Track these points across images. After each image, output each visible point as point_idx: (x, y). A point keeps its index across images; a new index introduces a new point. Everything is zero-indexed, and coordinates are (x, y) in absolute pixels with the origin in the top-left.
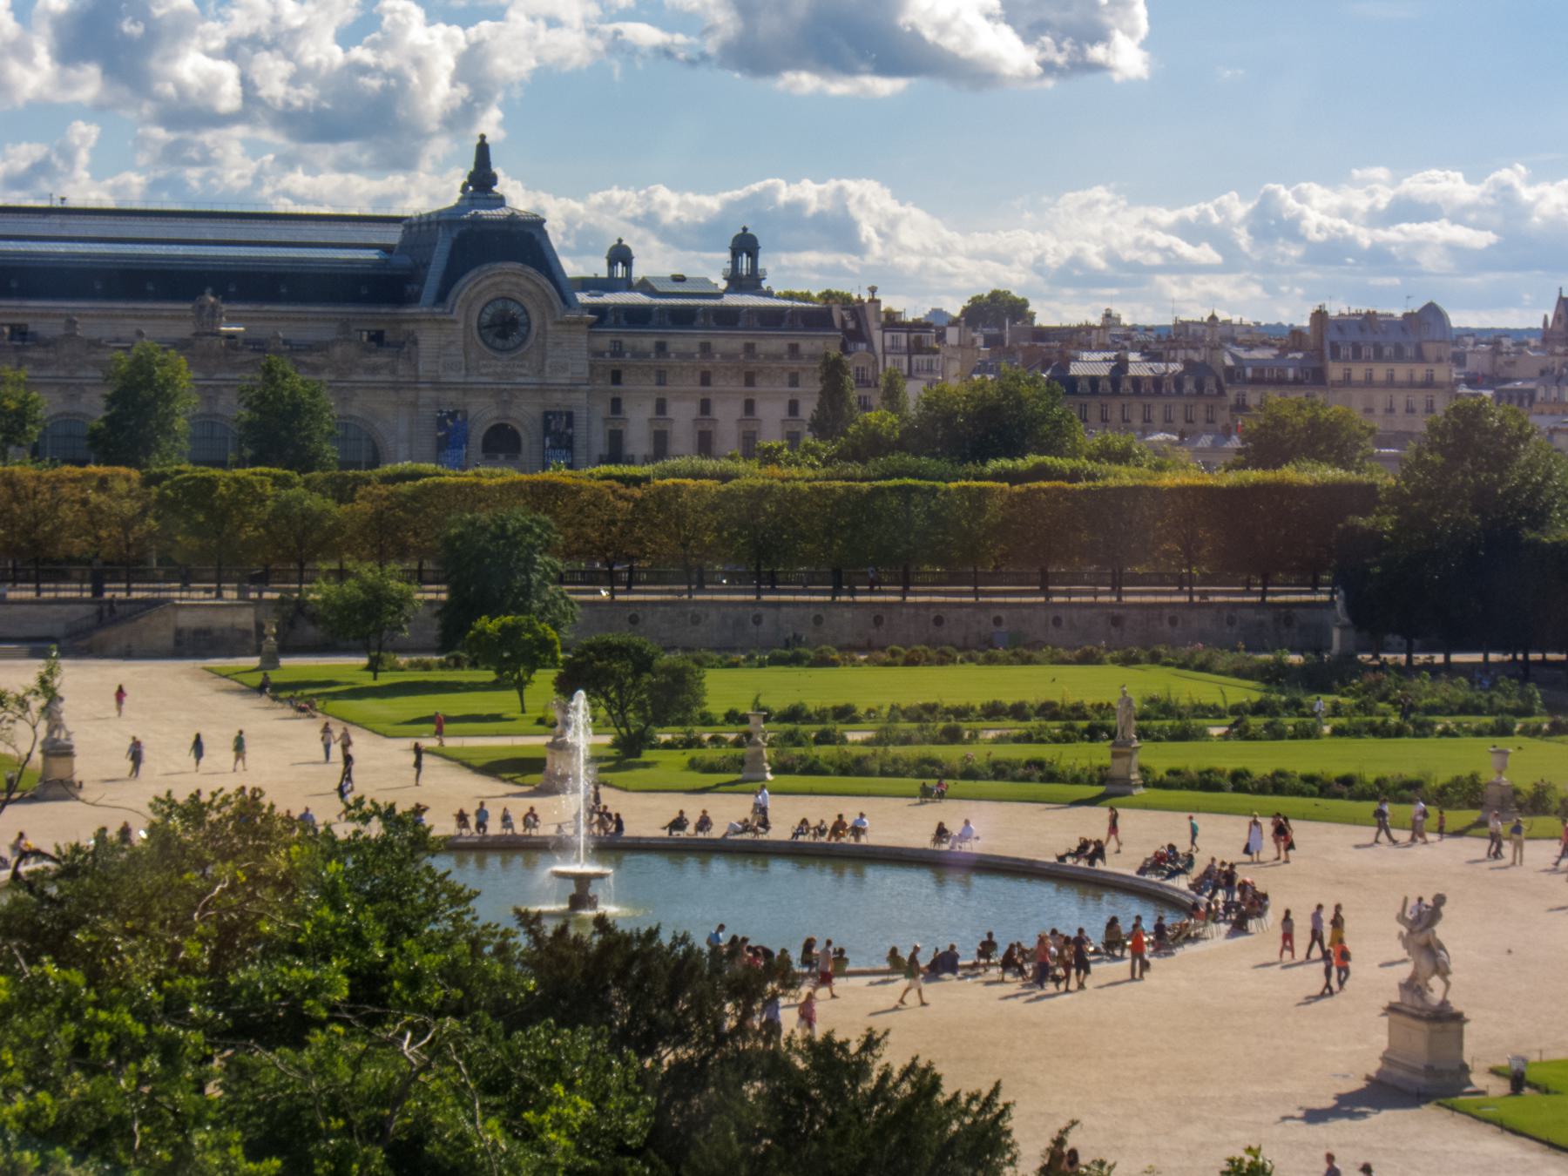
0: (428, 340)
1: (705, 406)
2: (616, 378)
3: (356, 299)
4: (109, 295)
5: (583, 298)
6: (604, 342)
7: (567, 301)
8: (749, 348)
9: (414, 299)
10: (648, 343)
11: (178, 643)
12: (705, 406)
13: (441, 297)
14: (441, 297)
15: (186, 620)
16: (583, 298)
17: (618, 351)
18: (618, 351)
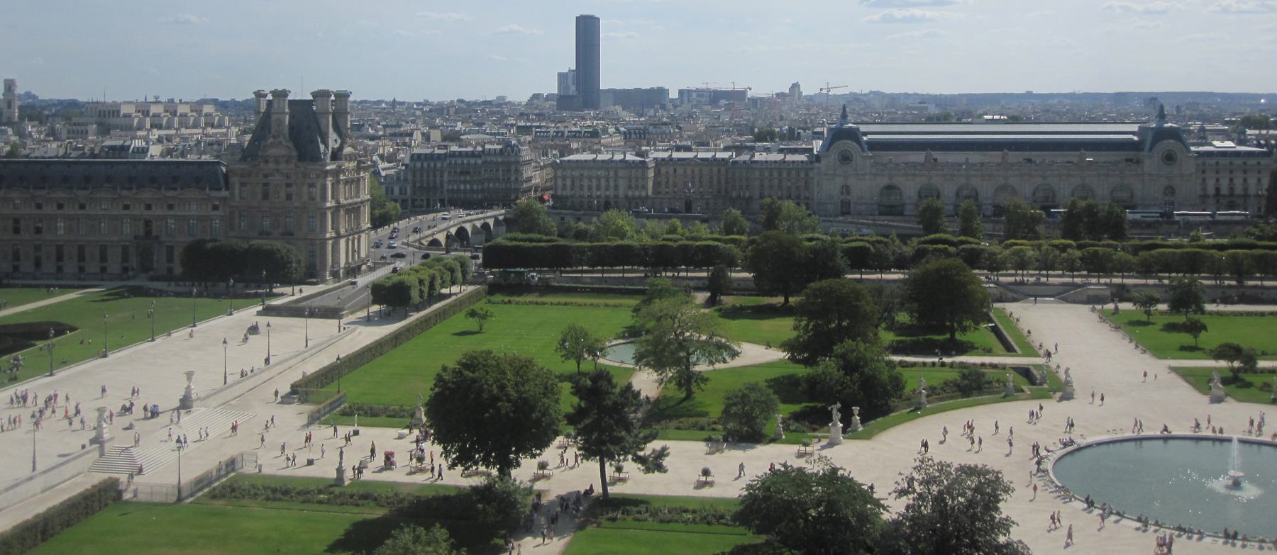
0: (1147, 162)
1: (1231, 180)
2: (1204, 172)
3: (1124, 150)
4: (1054, 150)
5: (1193, 149)
6: (1200, 162)
7: (1189, 151)
8: (1245, 163)
9: (1142, 150)
10: (1213, 162)
11: (1088, 299)
12: (1231, 180)
13: (1151, 150)
14: (1151, 150)
15: (1091, 293)
16: (1193, 149)
17: (1204, 164)
18: (1204, 164)
